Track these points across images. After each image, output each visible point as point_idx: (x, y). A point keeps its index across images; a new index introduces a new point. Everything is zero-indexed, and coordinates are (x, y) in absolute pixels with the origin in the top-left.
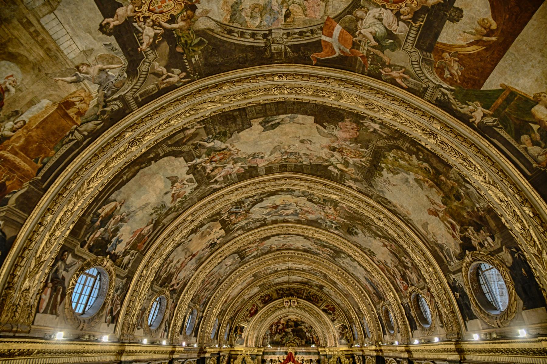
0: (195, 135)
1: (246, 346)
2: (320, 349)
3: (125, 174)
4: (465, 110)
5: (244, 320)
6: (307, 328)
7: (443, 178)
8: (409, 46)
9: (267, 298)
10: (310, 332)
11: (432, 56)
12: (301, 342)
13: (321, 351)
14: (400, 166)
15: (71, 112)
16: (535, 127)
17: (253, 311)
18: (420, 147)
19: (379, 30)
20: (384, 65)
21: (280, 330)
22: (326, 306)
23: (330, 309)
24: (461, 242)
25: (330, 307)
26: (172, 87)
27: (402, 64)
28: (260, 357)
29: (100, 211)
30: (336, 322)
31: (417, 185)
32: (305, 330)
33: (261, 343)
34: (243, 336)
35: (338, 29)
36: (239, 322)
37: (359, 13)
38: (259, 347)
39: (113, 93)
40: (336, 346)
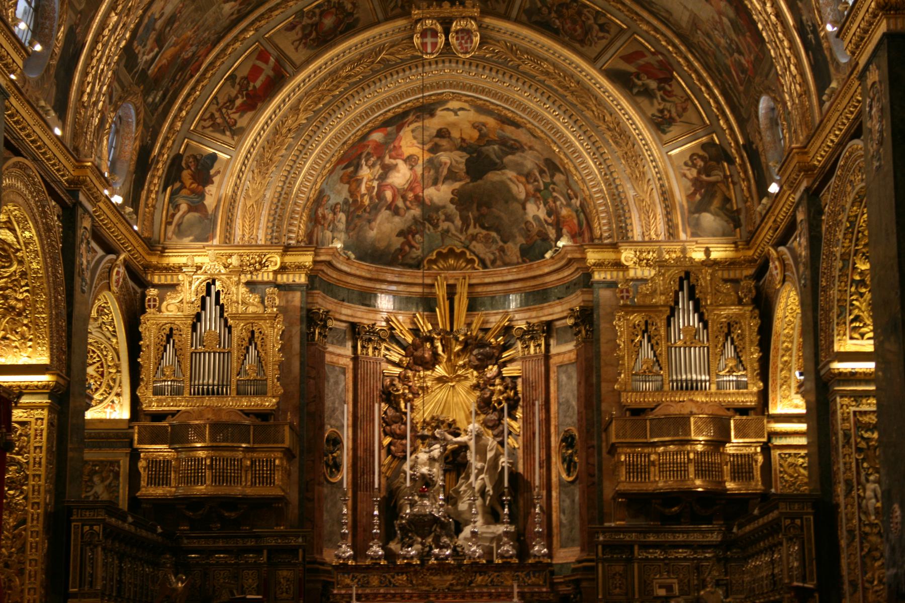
1: (227, 239)
2: (592, 257)
5: (216, 127)
6: (528, 176)
9: (328, 21)
10: (540, 195)
12: (502, 250)
13: (600, 265)
17: (258, 84)
21: (401, 193)
22: (628, 59)
23: (647, 70)
25: (649, 59)
28: (297, 298)
30: (674, 130)
32: (520, 190)
33: (299, 229)
34: (210, 202)
36: (189, 134)
38: (287, 249)
40: (672, 234)
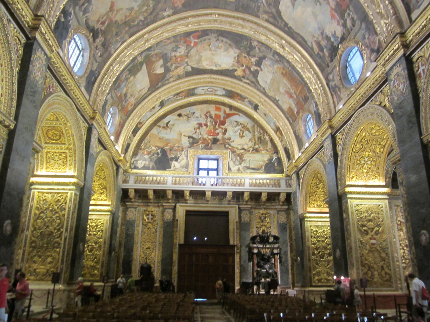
0: (266, 12)
3: (299, 40)
4: (143, 55)
7: (127, 29)
8: (169, 52)
11: (161, 55)
14: (143, 5)
15: (284, 72)
16: (129, 76)
18: (144, 26)
19: (179, 50)
20: (174, 42)
24: (96, 29)
26: (259, 42)
27: (168, 46)
29: (316, 53)
31: (131, 6)
35: (192, 44)
37: (187, 51)
39: (273, 60)
